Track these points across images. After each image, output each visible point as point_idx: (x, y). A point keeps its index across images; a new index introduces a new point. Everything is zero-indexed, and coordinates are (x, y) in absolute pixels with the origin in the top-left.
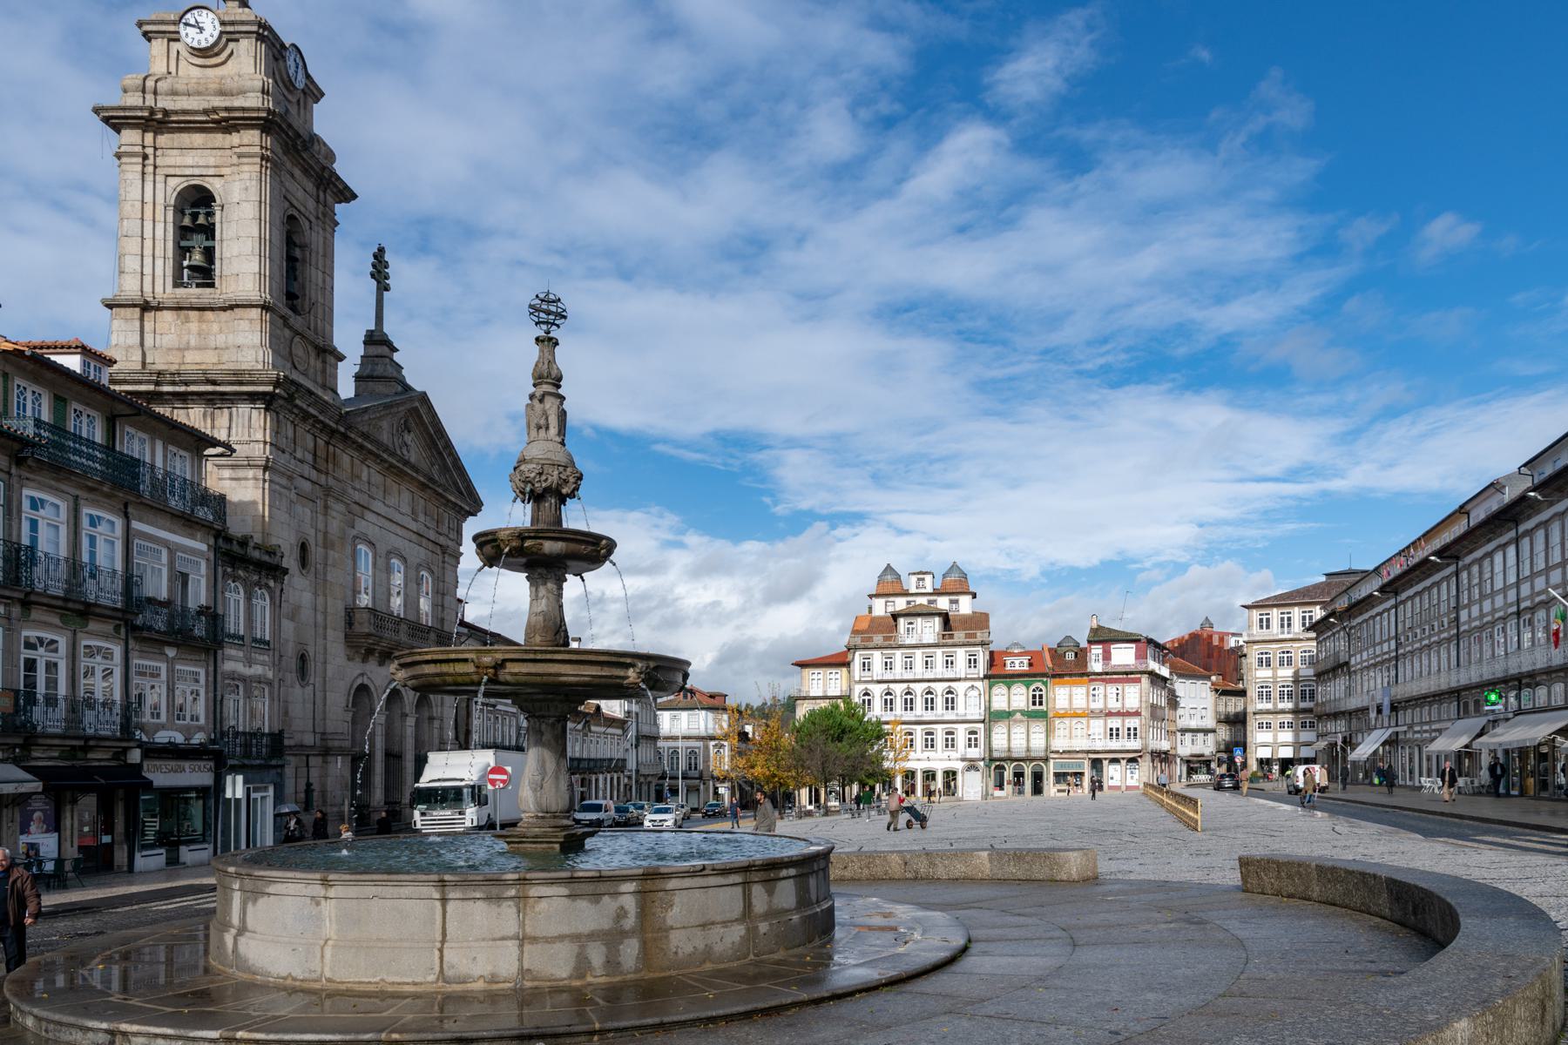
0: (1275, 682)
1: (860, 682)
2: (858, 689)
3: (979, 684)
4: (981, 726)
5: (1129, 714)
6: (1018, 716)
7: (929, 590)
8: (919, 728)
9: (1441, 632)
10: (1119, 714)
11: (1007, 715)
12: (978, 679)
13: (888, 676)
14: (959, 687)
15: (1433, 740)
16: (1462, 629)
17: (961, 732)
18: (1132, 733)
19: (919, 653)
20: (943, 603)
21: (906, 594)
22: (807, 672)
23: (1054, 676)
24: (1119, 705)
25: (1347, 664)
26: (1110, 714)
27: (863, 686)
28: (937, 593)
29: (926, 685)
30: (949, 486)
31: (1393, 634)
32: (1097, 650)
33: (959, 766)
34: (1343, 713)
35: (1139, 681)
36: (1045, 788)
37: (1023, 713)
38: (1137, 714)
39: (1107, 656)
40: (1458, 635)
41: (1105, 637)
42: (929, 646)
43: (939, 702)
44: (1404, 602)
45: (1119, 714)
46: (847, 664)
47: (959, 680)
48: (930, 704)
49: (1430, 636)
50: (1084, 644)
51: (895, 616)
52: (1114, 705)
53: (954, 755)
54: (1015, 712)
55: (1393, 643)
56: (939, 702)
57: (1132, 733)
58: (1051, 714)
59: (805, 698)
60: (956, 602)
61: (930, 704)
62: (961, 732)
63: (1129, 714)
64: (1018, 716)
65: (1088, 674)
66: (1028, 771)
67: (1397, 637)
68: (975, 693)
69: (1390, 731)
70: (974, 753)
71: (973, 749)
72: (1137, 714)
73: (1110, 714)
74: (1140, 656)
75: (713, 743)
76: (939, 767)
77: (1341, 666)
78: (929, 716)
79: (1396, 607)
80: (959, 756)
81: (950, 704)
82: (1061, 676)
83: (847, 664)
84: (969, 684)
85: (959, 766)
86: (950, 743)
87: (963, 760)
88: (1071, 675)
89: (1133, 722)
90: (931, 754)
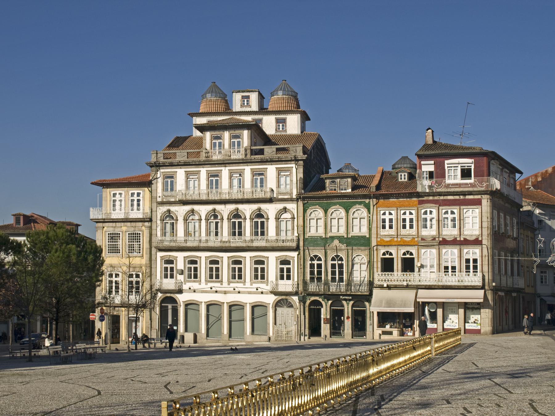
1: (162, 203)
3: (292, 206)
4: (295, 254)
5: (466, 242)
6: (336, 242)
8: (225, 255)
10: (454, 242)
12: (291, 200)
14: (271, 210)
17: (272, 259)
18: (470, 266)
19: (225, 171)
22: (108, 193)
23: (377, 197)
24: (455, 232)
26: (445, 242)
27: (164, 209)
29: (232, 207)
32: (428, 166)
35: (478, 203)
36: (369, 328)
37: (341, 239)
38: (477, 242)
41: (439, 153)
43: (248, 226)
45: (454, 242)
46: (147, 184)
47: (270, 201)
48: (237, 230)
50: (415, 160)
52: (449, 232)
53: (263, 287)
54: (333, 238)
56: (248, 226)
57: (470, 266)
58: (374, 243)
59: (104, 221)
60: (284, 121)
61: (237, 230)
62: (272, 259)
63: (466, 242)
64: (336, 242)
65: (418, 195)
66: (348, 308)
68: (287, 216)
70: (286, 286)
71: (285, 281)
72: (477, 242)
73: (445, 242)
76: (248, 300)
78: (237, 242)
80: (269, 288)
81: (260, 229)
82: (387, 197)
84: (280, 206)
85: (271, 299)
86: (260, 274)
88: (398, 196)
89: (473, 253)
90: (239, 286)
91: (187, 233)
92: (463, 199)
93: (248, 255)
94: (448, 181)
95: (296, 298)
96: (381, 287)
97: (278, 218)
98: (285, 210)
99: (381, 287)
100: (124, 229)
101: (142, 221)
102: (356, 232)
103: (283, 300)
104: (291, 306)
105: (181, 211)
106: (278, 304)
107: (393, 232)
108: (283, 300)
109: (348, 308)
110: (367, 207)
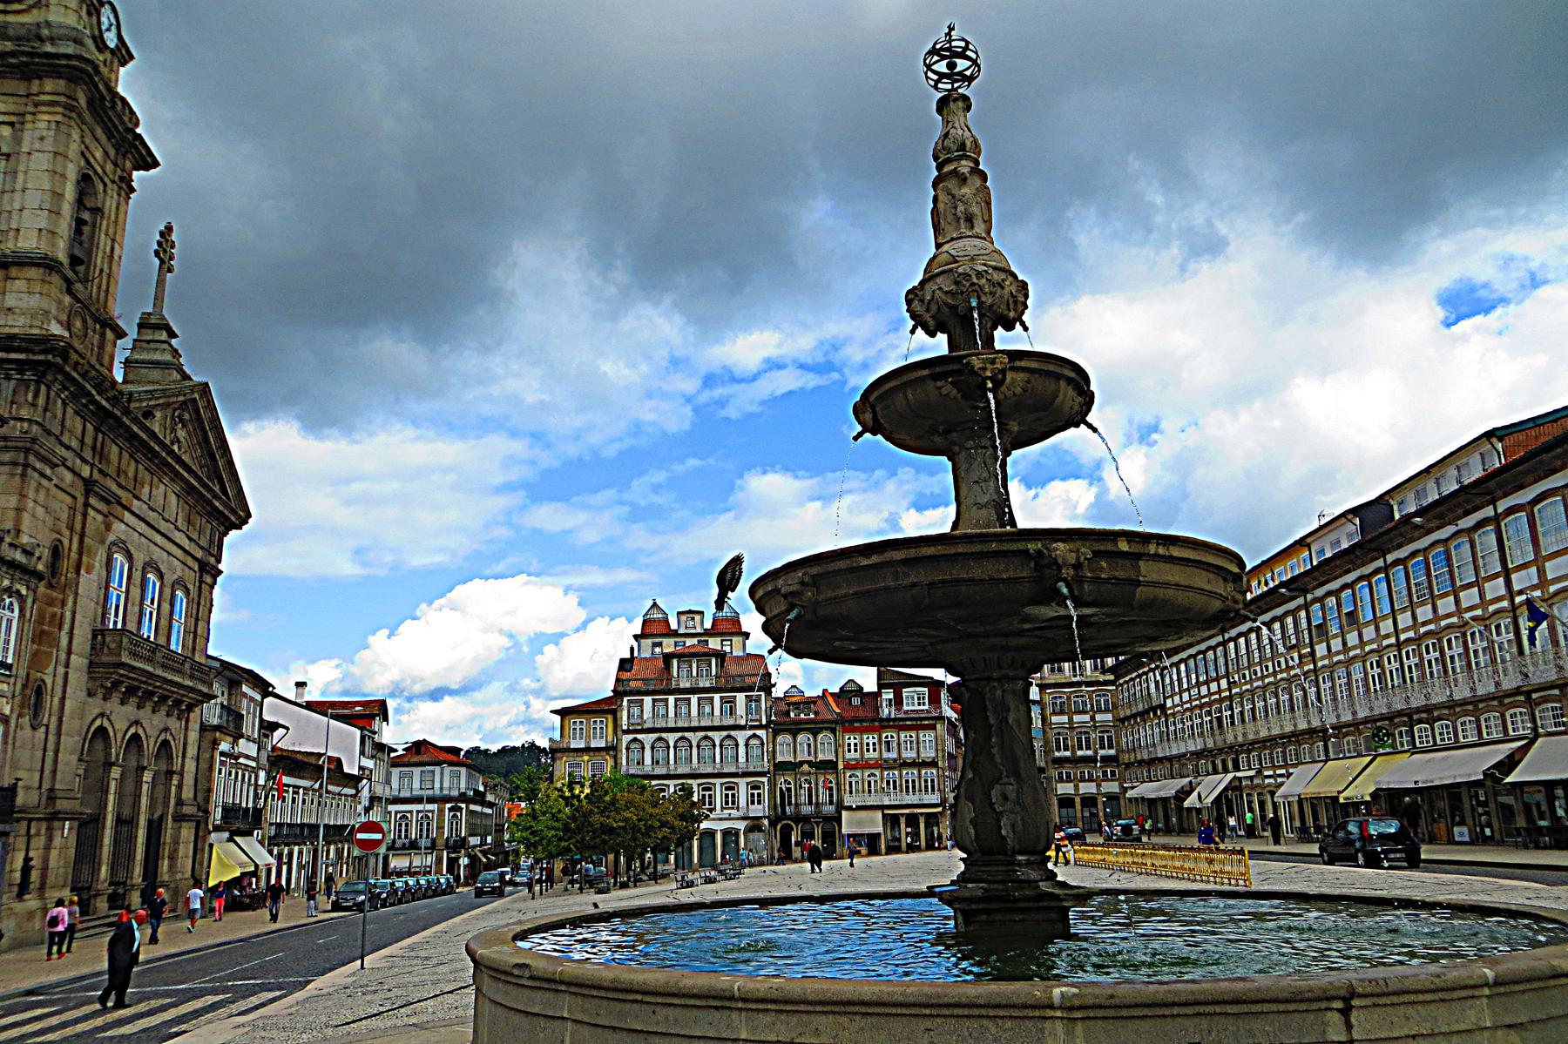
0: (1072, 728)
1: (627, 732)
2: (626, 738)
4: (765, 779)
5: (925, 764)
6: (806, 767)
7: (699, 630)
9: (1289, 668)
10: (914, 764)
11: (793, 767)
12: (760, 727)
13: (661, 724)
14: (741, 736)
15: (1282, 784)
16: (1320, 664)
20: (714, 643)
21: (675, 634)
24: (913, 754)
25: (1163, 707)
26: (906, 764)
27: (631, 737)
28: (707, 633)
30: (727, 510)
31: (1222, 671)
32: (888, 695)
33: (741, 826)
34: (1161, 760)
35: (933, 727)
37: (809, 763)
38: (933, 764)
39: (898, 701)
40: (1315, 671)
42: (705, 690)
44: (1235, 639)
45: (914, 764)
49: (1275, 673)
51: (668, 658)
52: (909, 755)
53: (734, 813)
55: (1224, 683)
58: (841, 766)
63: (925, 764)
64: (806, 767)
67: (1227, 675)
69: (1230, 776)
70: (757, 810)
72: (933, 764)
73: (906, 764)
74: (935, 700)
75: (449, 805)
77: (1154, 709)
79: (1224, 644)
80: (740, 814)
83: (614, 713)
84: (750, 733)
85: (741, 826)
87: (744, 818)
91: (655, 762)
92: (918, 723)
93: (718, 781)
94: (905, 708)
95: (766, 822)
96: (850, 808)
97: (747, 745)
98: (755, 736)
99: (850, 808)
100: (586, 758)
101: (606, 749)
102: (821, 757)
103: (754, 826)
104: (760, 830)
105: (648, 739)
106: (749, 830)
107: (857, 755)
108: (754, 826)
109: (818, 832)
110: (833, 731)
